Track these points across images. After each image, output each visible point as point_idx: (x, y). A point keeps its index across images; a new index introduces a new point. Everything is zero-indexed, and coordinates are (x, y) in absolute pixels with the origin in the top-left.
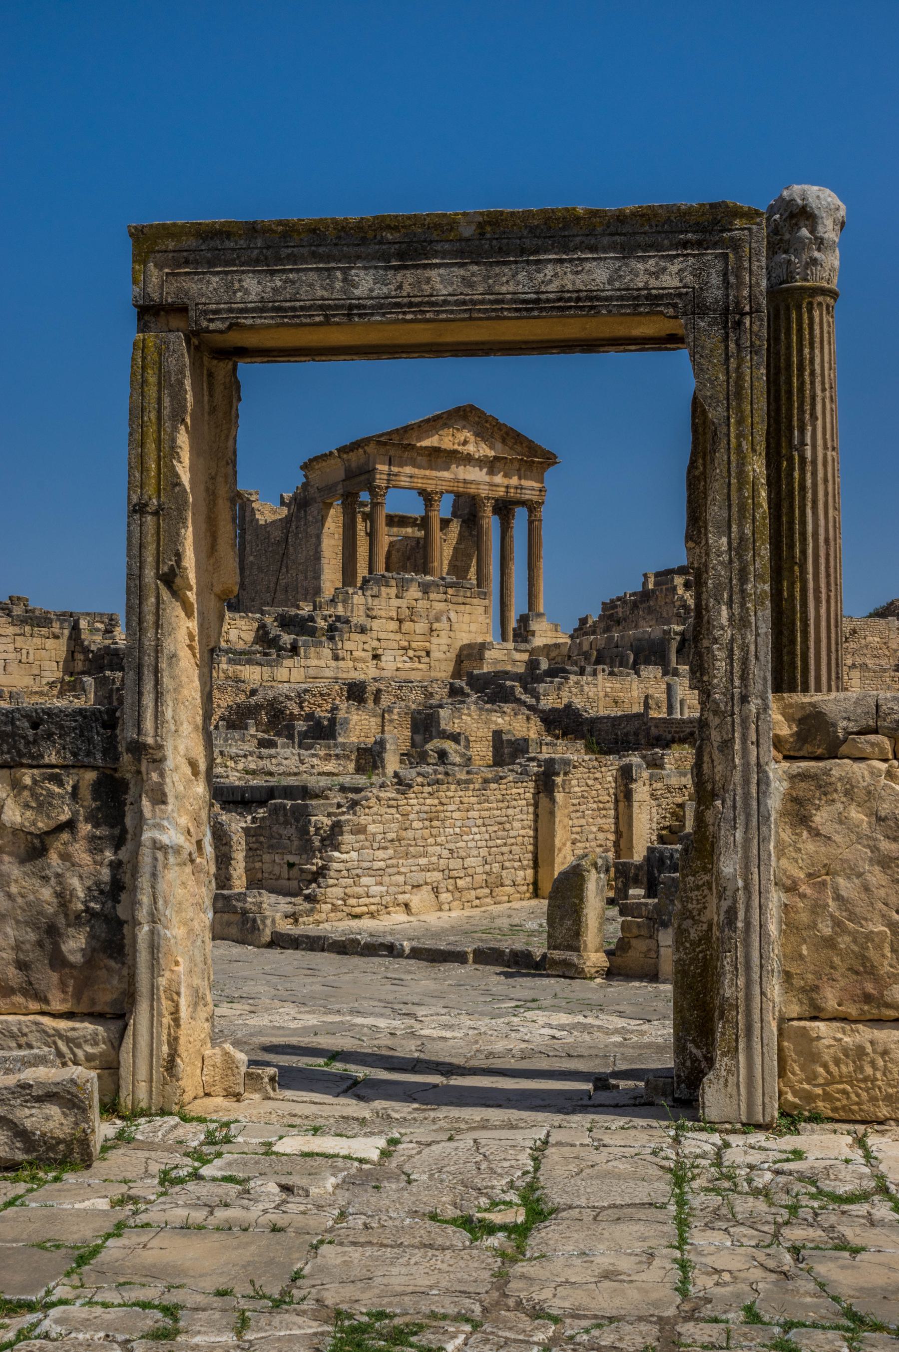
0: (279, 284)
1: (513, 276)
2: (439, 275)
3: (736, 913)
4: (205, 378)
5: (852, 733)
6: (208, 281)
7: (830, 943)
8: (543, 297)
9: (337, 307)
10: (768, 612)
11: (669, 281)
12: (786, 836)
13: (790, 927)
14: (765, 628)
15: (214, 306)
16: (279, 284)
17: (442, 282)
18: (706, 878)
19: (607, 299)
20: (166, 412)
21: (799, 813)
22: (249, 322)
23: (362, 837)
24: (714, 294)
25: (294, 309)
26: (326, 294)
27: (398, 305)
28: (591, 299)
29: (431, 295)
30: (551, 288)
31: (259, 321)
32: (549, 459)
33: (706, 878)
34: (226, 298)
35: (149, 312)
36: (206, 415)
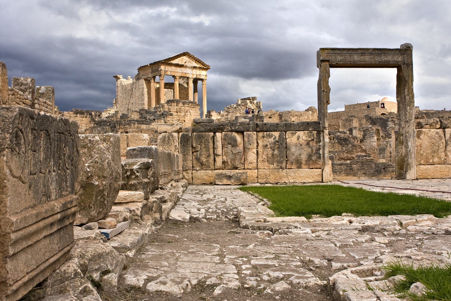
7: (422, 154)
11: (400, 59)
12: (417, 139)
13: (417, 152)
21: (418, 137)
24: (406, 61)
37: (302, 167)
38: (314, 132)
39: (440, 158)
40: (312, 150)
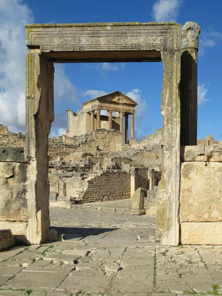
0: (62, 41)
2: (102, 39)
6: (45, 40)
8: (127, 45)
9: (77, 47)
15: (46, 46)
16: (62, 41)
17: (103, 41)
22: (55, 50)
25: (66, 47)
26: (74, 44)
27: (91, 46)
31: (57, 50)
40: (12, 193)
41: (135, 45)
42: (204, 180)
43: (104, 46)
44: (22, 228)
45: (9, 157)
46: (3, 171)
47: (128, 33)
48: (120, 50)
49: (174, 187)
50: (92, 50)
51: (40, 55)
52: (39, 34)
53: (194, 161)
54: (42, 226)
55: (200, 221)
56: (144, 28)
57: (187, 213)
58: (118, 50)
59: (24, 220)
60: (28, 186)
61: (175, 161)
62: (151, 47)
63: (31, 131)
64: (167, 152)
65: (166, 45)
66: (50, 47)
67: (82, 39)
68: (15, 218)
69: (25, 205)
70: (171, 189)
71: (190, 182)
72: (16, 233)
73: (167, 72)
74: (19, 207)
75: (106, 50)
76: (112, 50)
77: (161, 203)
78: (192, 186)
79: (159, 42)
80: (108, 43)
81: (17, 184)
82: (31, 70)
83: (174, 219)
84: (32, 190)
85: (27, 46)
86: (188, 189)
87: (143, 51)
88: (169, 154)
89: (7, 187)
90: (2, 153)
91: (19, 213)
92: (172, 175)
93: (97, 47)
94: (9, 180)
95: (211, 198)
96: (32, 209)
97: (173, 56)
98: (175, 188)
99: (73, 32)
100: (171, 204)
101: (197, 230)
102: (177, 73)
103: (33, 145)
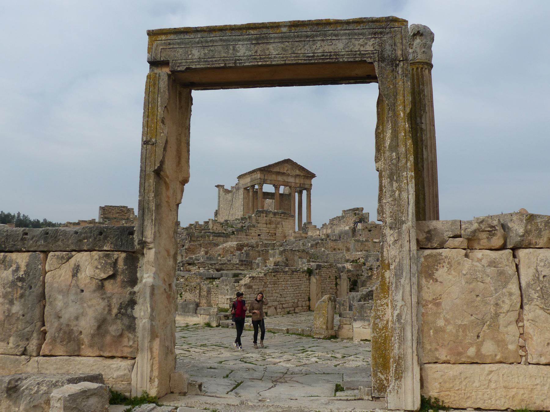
1: (303, 47)
2: (273, 47)
3: (401, 316)
4: (178, 95)
5: (450, 237)
8: (316, 55)
9: (230, 60)
10: (414, 185)
11: (369, 48)
14: (412, 191)
15: (179, 61)
16: (207, 52)
18: (385, 301)
19: (343, 55)
20: (159, 104)
22: (194, 67)
23: (251, 290)
25: (212, 61)
26: (226, 55)
27: (255, 59)
28: (336, 55)
29: (269, 55)
30: (319, 51)
31: (198, 67)
32: (313, 176)
33: (385, 301)
34: (185, 58)
35: (154, 63)
36: (178, 110)
37: (82, 353)
38: (116, 255)
39: (501, 343)
41: (329, 54)
42: (463, 283)
43: (276, 58)
44: (125, 370)
45: (108, 243)
46: (97, 268)
47: (317, 36)
48: (303, 62)
49: (407, 297)
50: (256, 63)
51: (169, 76)
52: (170, 44)
53: (443, 248)
54: (160, 368)
55: (461, 362)
56: (344, 28)
57: (434, 345)
58: (300, 62)
59: (128, 355)
60: (139, 294)
61: (407, 248)
62: (358, 56)
63: (149, 197)
64: (392, 232)
65: (384, 53)
66: (186, 62)
67: (239, 47)
68: (114, 351)
69: (131, 327)
70: (403, 300)
71: (437, 288)
72: (113, 378)
73: (387, 94)
74: (120, 331)
75: (279, 63)
76: (290, 62)
77: (380, 326)
78: (441, 295)
79: (372, 49)
80: (284, 53)
81: (120, 289)
82: (154, 99)
83: (409, 357)
84: (145, 300)
85: (149, 62)
86: (434, 299)
87: (344, 62)
88: (396, 235)
89: (102, 295)
90: (97, 235)
91: (120, 342)
92: (402, 273)
93: (263, 59)
94: (107, 284)
95: (480, 316)
96: (143, 336)
97: (396, 68)
98: (410, 297)
99: (224, 38)
100: (403, 329)
101: (455, 379)
102: (404, 97)
103: (150, 221)
